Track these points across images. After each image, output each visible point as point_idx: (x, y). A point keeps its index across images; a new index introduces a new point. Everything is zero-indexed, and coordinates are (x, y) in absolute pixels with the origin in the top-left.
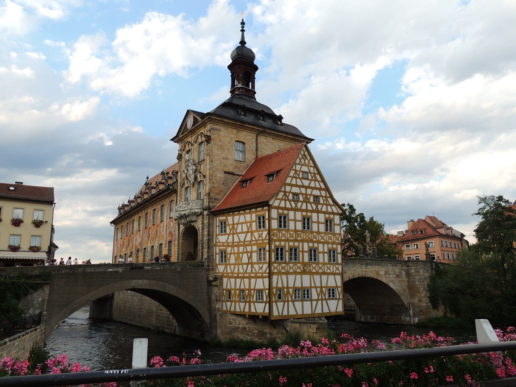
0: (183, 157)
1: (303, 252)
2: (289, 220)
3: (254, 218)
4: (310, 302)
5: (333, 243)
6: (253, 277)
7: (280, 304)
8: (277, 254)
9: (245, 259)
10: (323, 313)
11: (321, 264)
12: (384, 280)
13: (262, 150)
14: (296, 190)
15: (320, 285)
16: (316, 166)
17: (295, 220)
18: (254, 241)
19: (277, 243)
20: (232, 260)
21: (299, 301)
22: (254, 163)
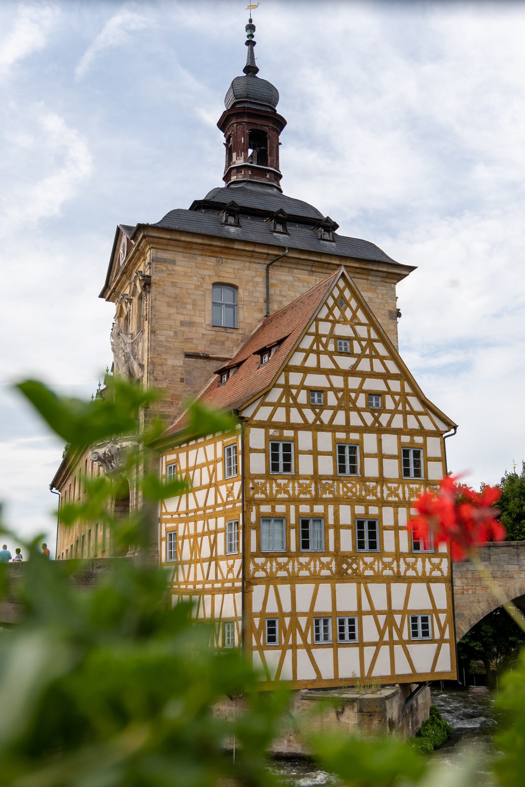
1: (337, 527)
2: (298, 452)
3: (220, 455)
4: (356, 650)
10: (393, 675)
11: (388, 555)
13: (280, 299)
14: (316, 381)
15: (385, 607)
16: (372, 323)
17: (315, 453)
19: (265, 509)
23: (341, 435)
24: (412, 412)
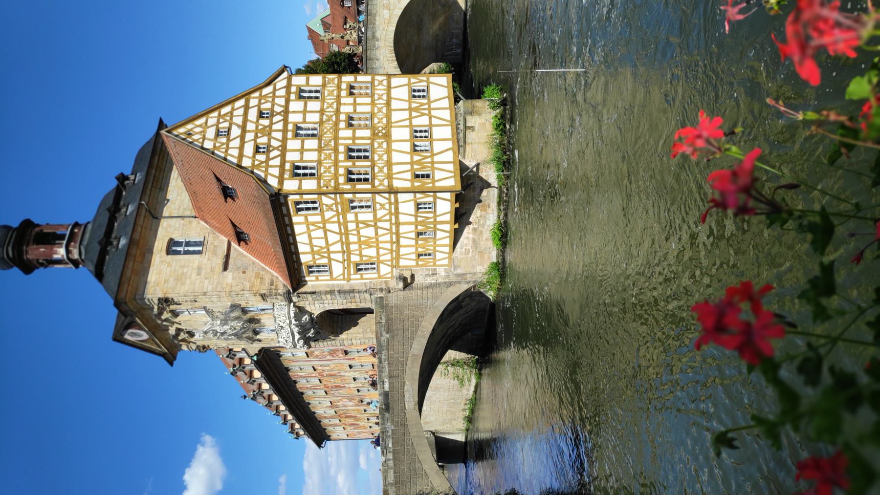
0: (200, 343)
1: (354, 138)
4: (434, 129)
5: (339, 88)
6: (397, 218)
7: (438, 175)
8: (359, 180)
9: (369, 232)
10: (450, 108)
11: (373, 109)
12: (399, 12)
13: (181, 210)
15: (407, 113)
18: (339, 219)
19: (342, 180)
20: (371, 252)
21: (431, 144)
22: (206, 222)
23: (290, 135)
24: (274, 92)
